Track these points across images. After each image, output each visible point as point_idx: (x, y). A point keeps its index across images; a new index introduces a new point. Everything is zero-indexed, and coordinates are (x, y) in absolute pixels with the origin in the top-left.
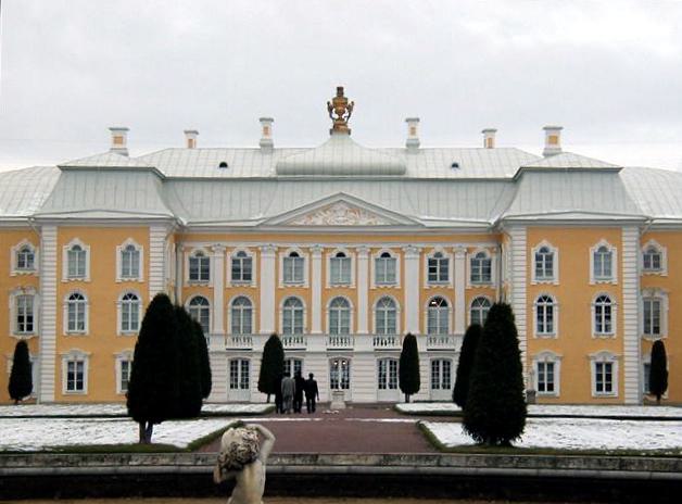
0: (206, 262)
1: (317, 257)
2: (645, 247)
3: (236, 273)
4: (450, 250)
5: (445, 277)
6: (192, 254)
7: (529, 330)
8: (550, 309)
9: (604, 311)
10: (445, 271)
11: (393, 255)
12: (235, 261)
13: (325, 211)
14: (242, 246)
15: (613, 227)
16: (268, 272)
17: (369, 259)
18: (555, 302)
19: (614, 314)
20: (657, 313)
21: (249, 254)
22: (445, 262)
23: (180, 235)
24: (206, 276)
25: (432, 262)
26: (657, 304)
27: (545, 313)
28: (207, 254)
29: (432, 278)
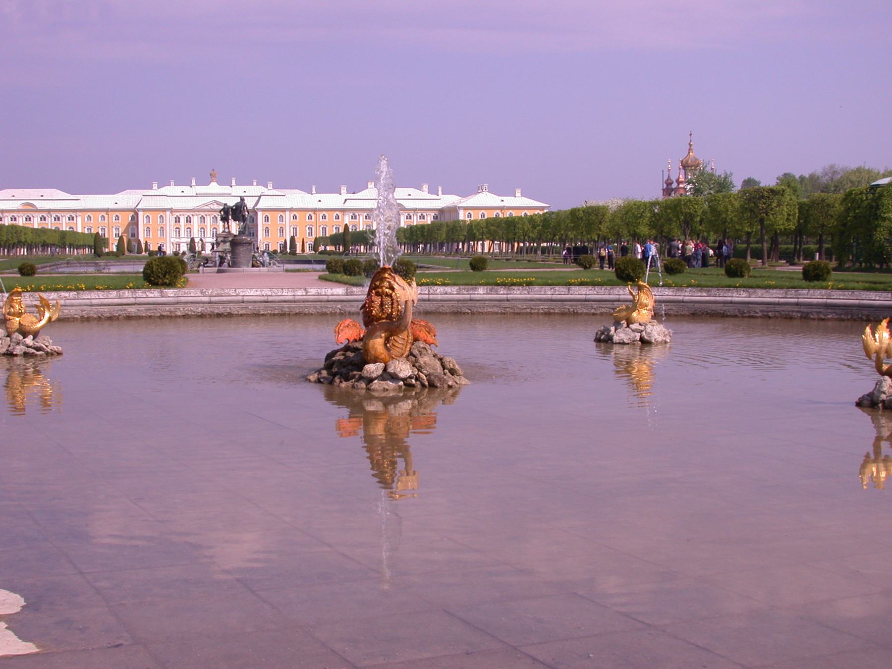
0: (179, 218)
2: (293, 215)
3: (187, 221)
6: (175, 216)
9: (282, 230)
12: (187, 218)
13: (210, 204)
14: (189, 214)
15: (284, 210)
16: (196, 220)
18: (270, 228)
19: (284, 230)
20: (296, 231)
21: (191, 216)
23: (172, 210)
24: (179, 222)
26: (296, 229)
27: (267, 230)
28: (179, 216)
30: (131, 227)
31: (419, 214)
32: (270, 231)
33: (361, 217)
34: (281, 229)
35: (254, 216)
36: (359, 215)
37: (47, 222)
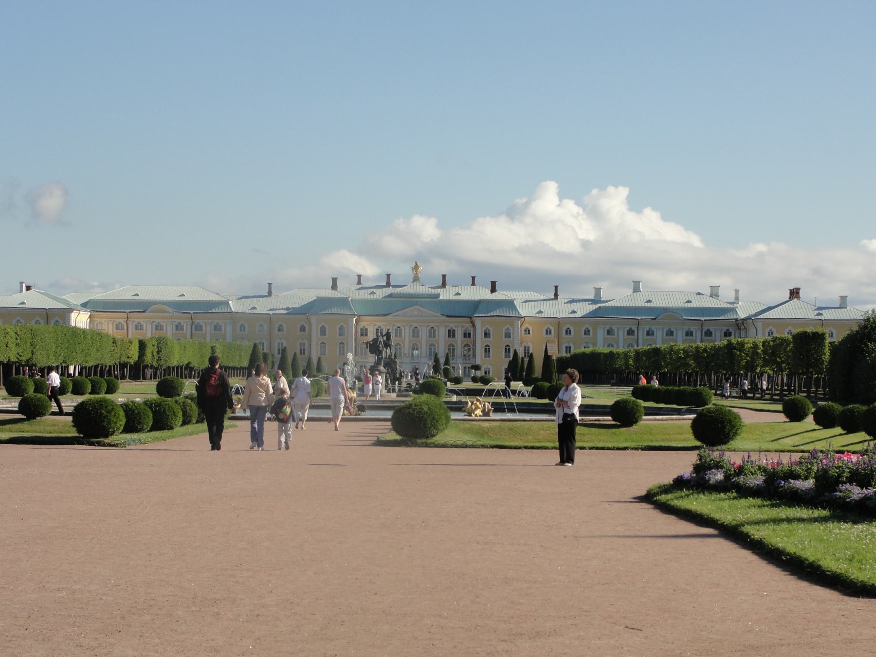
0: (366, 330)
1: (407, 328)
4: (456, 327)
5: (454, 336)
6: (361, 327)
7: (481, 357)
8: (489, 349)
10: (454, 334)
11: (435, 328)
12: (377, 330)
17: (426, 329)
22: (454, 331)
25: (449, 331)
27: (487, 350)
28: (366, 327)
29: (449, 336)
30: (301, 341)
31: (705, 329)
32: (491, 349)
33: (621, 333)
34: (508, 348)
35: (470, 328)
36: (618, 329)
37: (185, 332)
